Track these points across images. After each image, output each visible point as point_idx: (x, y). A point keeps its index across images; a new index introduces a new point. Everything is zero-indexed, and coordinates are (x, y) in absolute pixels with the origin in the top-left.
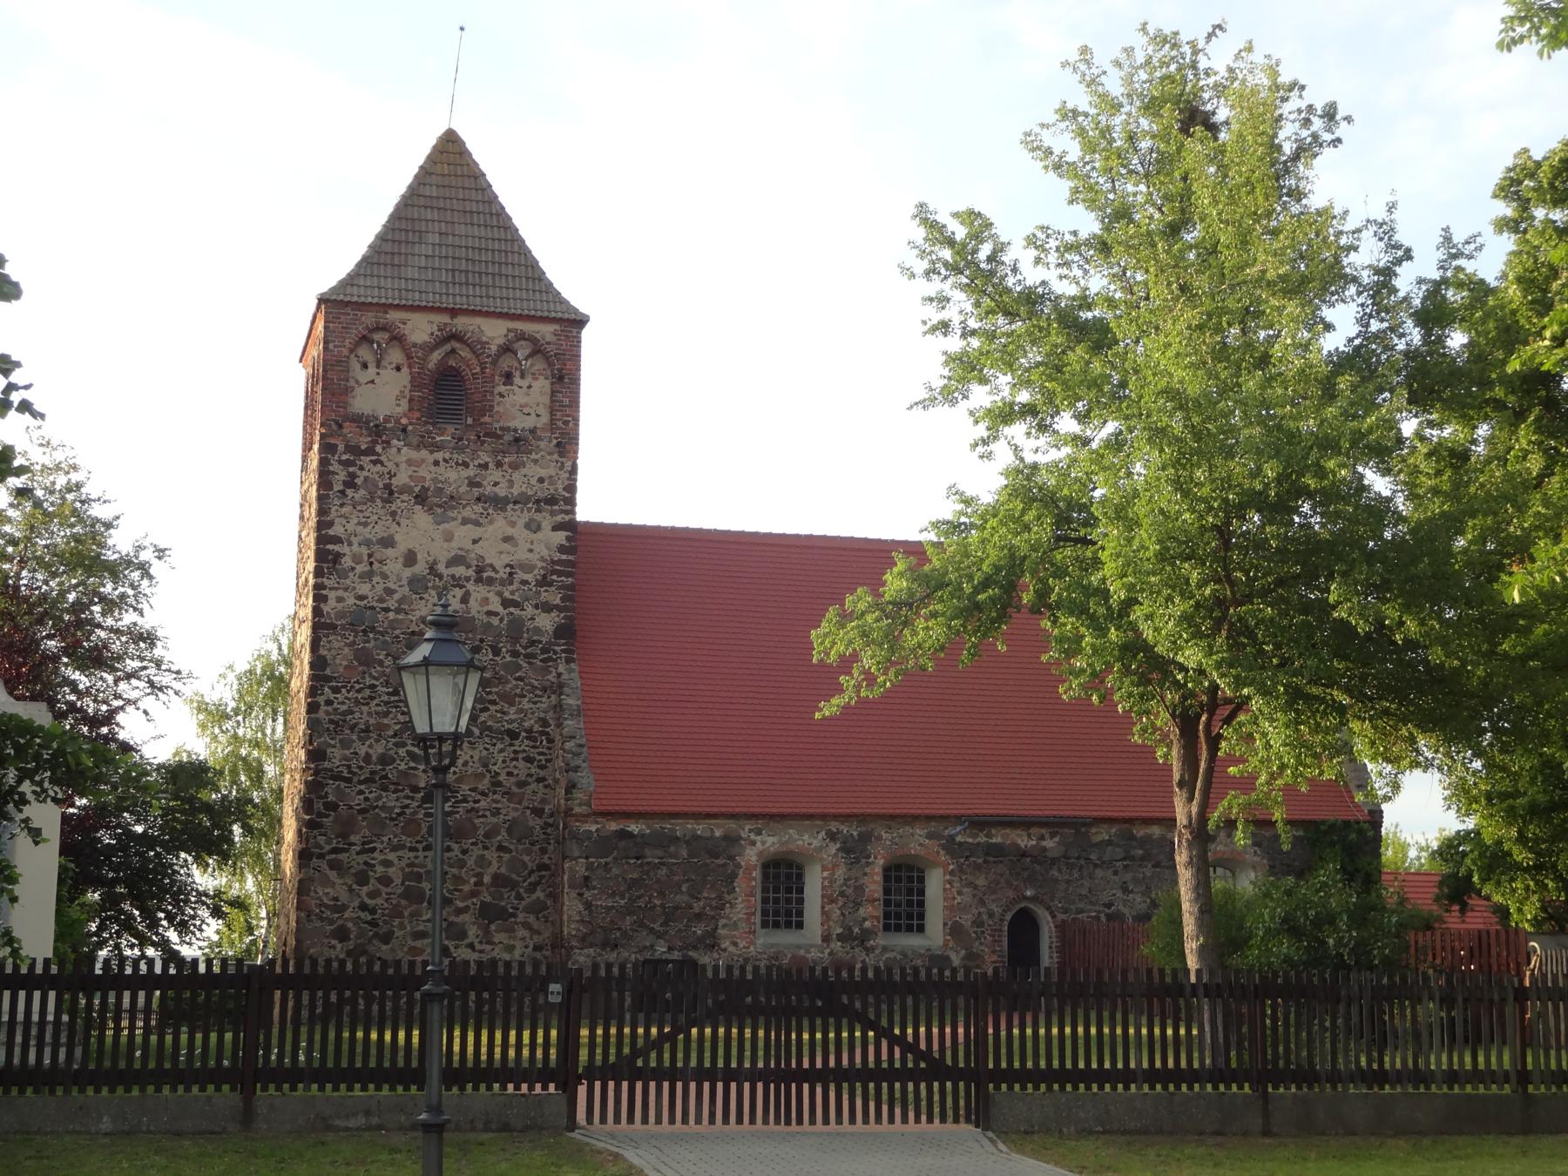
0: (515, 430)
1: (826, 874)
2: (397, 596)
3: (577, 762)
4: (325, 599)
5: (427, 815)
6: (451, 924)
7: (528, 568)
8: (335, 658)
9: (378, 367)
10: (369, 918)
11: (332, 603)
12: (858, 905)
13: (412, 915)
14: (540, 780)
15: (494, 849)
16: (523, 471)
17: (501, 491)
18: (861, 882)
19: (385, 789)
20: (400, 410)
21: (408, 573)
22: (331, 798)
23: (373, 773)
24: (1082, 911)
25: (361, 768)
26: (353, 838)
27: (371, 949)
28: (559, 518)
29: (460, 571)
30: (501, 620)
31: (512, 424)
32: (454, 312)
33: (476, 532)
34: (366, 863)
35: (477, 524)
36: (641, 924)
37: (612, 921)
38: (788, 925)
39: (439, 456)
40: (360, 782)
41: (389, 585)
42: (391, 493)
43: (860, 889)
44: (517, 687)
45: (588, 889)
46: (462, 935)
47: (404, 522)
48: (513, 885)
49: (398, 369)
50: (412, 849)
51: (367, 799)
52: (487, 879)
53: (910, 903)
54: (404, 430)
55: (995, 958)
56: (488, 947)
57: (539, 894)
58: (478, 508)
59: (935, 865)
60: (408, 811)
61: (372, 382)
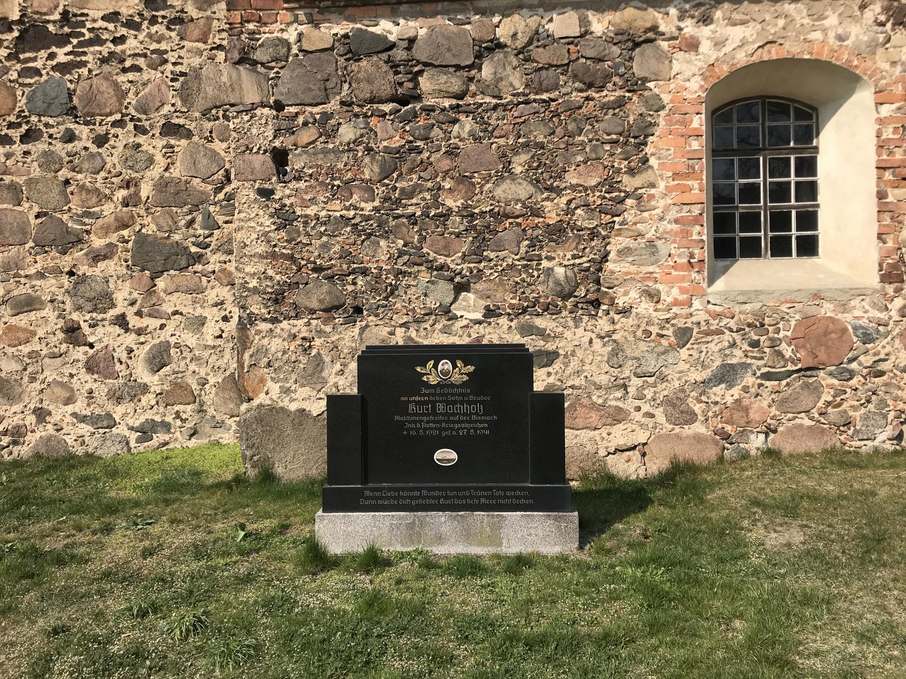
6: (84, 279)
15: (157, 132)
46: (103, 301)
56: (154, 323)
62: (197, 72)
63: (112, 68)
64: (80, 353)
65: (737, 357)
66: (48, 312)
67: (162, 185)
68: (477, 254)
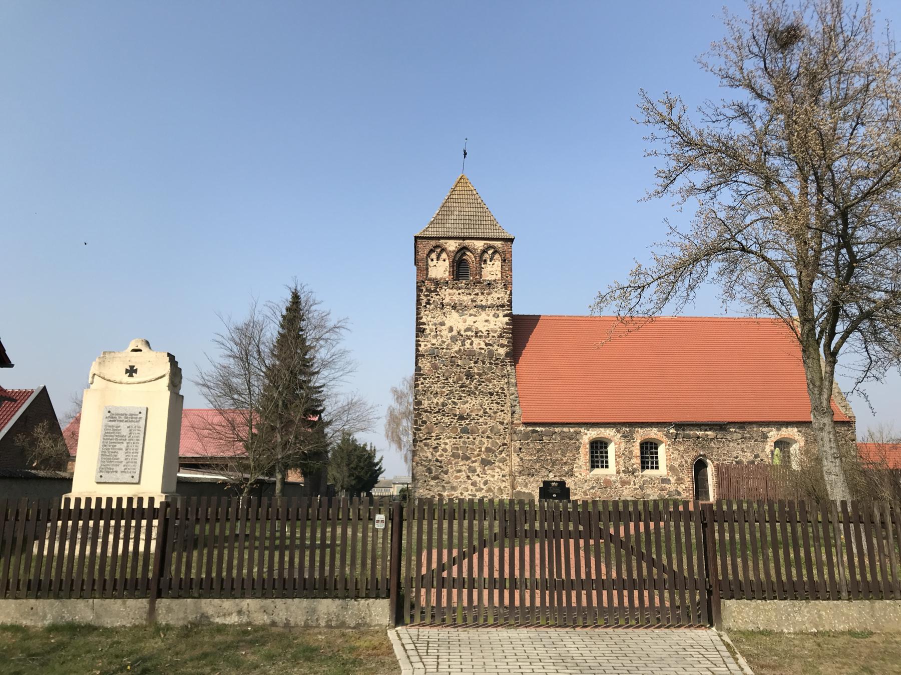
0: (488, 280)
1: (616, 446)
2: (446, 344)
3: (516, 403)
4: (420, 345)
5: (459, 425)
6: (470, 467)
7: (496, 331)
8: (424, 367)
9: (437, 260)
10: (439, 464)
11: (423, 346)
12: (630, 459)
13: (455, 463)
14: (502, 411)
16: (492, 295)
17: (484, 303)
18: (631, 449)
19: (444, 416)
20: (445, 275)
21: (450, 335)
22: (424, 419)
23: (439, 409)
24: (725, 460)
25: (435, 408)
26: (433, 434)
27: (440, 476)
28: (506, 312)
29: (469, 333)
30: (485, 351)
31: (487, 279)
32: (464, 239)
33: (475, 319)
34: (437, 444)
35: (475, 316)
36: (543, 467)
37: (531, 466)
38: (602, 467)
39: (460, 291)
40: (435, 413)
41: (443, 339)
42: (443, 306)
43: (631, 452)
44: (492, 376)
45: (521, 453)
46: (474, 471)
47: (448, 316)
48: (494, 452)
49: (444, 260)
50: (455, 438)
51: (437, 419)
52: (483, 449)
53: (652, 458)
54: (447, 282)
55: (689, 480)
56: (485, 476)
57: (503, 455)
58: (475, 310)
59: (662, 442)
60: (453, 424)
61: (435, 266)
62: (493, 426)
63: (477, 425)
64: (470, 481)
65: (594, 485)
66: (463, 473)
67: (487, 448)
68: (552, 466)
